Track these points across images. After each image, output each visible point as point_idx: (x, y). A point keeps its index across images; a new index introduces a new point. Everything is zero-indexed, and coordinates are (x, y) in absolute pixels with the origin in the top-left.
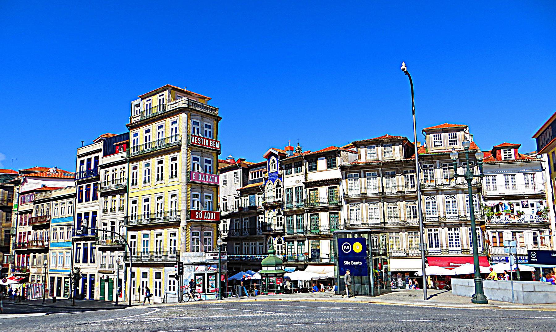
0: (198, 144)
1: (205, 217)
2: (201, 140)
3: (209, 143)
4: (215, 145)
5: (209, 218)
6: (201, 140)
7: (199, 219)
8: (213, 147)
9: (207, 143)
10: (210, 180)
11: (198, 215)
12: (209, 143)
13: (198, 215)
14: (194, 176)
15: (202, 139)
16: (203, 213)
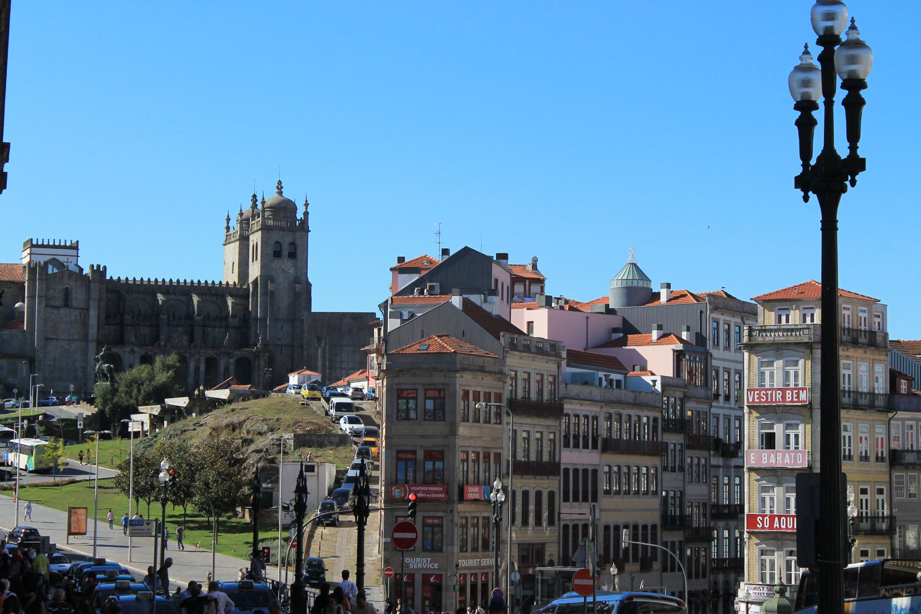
0: (760, 402)
1: (776, 525)
2: (767, 395)
3: (784, 397)
4: (798, 397)
5: (784, 527)
6: (767, 395)
7: (763, 527)
8: (792, 401)
9: (779, 396)
10: (787, 460)
11: (762, 522)
12: (784, 397)
13: (762, 522)
14: (752, 458)
15: (769, 392)
16: (772, 518)
